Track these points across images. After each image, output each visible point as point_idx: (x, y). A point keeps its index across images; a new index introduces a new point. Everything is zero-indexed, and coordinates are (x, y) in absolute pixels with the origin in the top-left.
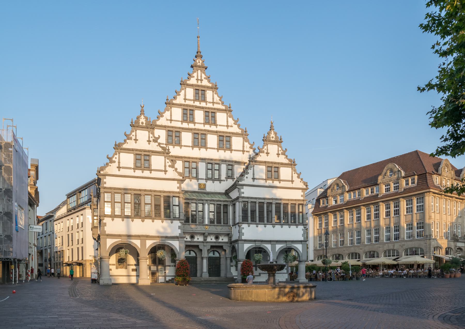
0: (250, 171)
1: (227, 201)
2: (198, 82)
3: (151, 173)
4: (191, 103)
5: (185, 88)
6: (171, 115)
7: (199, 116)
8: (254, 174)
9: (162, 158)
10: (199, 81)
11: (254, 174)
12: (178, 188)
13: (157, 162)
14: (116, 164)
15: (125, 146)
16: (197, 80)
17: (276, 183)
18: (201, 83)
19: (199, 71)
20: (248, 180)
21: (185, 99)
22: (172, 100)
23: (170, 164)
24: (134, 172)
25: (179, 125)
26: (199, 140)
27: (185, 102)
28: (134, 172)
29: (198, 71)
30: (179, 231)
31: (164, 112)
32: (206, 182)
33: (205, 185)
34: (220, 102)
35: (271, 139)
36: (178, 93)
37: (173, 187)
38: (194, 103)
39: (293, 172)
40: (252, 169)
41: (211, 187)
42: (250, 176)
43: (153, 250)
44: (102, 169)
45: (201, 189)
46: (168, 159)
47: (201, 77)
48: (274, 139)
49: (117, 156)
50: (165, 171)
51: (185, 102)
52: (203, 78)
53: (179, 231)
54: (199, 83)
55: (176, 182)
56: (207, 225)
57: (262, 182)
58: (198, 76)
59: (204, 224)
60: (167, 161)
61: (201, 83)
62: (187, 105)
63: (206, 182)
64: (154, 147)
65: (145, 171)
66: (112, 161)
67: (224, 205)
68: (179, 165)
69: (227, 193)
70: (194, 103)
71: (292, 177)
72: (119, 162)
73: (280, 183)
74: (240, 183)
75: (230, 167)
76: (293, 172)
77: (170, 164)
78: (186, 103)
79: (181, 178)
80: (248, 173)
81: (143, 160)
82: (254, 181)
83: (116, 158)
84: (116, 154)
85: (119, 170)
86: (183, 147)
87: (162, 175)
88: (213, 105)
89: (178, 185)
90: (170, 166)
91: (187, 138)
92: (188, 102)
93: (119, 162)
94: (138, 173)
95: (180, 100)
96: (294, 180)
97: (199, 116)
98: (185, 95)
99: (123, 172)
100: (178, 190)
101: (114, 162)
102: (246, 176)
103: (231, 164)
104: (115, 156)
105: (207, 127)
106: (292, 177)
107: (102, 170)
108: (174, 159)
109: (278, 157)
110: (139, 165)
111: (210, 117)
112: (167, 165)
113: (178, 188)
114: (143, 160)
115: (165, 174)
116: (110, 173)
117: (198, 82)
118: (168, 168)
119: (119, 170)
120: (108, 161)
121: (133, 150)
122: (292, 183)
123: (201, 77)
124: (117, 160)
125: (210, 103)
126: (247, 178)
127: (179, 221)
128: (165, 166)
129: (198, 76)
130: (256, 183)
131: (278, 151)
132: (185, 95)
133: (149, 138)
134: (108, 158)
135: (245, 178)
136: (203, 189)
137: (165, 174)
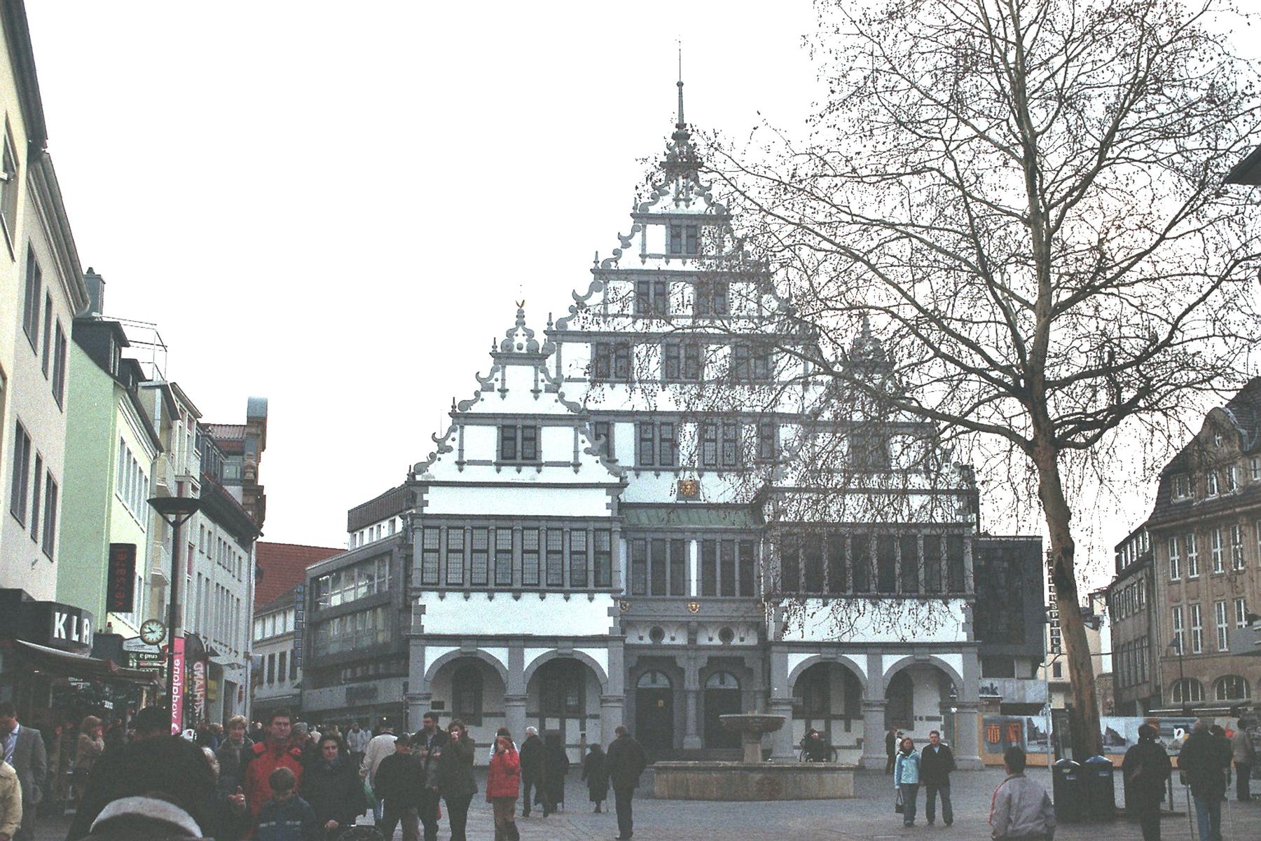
1: (750, 531)
3: (539, 471)
4: (661, 264)
5: (645, 227)
7: (681, 296)
9: (567, 432)
10: (682, 204)
12: (608, 506)
13: (556, 443)
14: (454, 456)
15: (475, 409)
18: (687, 206)
21: (644, 256)
22: (607, 261)
23: (588, 445)
24: (498, 471)
25: (625, 325)
26: (683, 361)
27: (644, 262)
28: (498, 471)
30: (610, 622)
31: (589, 296)
32: (700, 476)
33: (696, 485)
36: (625, 241)
37: (596, 505)
38: (667, 263)
41: (718, 489)
43: (544, 669)
44: (420, 468)
45: (688, 497)
46: (583, 433)
49: (456, 435)
50: (576, 466)
51: (644, 262)
53: (610, 622)
55: (604, 491)
56: (693, 600)
59: (687, 596)
60: (581, 437)
61: (687, 206)
62: (648, 272)
63: (700, 476)
64: (548, 404)
65: (524, 469)
66: (444, 449)
67: (743, 541)
68: (624, 437)
69: (755, 508)
70: (667, 263)
72: (461, 450)
75: (766, 431)
77: (588, 445)
78: (646, 267)
79: (617, 480)
81: (519, 442)
83: (454, 440)
84: (455, 430)
85: (461, 470)
87: (566, 475)
89: (609, 499)
90: (587, 451)
91: (649, 361)
92: (651, 265)
93: (461, 450)
94: (508, 474)
95: (630, 260)
97: (681, 296)
98: (644, 245)
99: (471, 474)
100: (608, 513)
101: (449, 449)
103: (768, 423)
104: (453, 435)
107: (420, 472)
108: (599, 427)
110: (509, 453)
111: (711, 293)
112: (582, 447)
113: (608, 506)
114: (519, 442)
115: (576, 472)
116: (438, 478)
118: (583, 458)
119: (461, 470)
120: (434, 448)
124: (455, 445)
127: (608, 596)
128: (576, 452)
132: (644, 245)
133: (536, 385)
134: (434, 439)
136: (692, 498)
137: (576, 472)
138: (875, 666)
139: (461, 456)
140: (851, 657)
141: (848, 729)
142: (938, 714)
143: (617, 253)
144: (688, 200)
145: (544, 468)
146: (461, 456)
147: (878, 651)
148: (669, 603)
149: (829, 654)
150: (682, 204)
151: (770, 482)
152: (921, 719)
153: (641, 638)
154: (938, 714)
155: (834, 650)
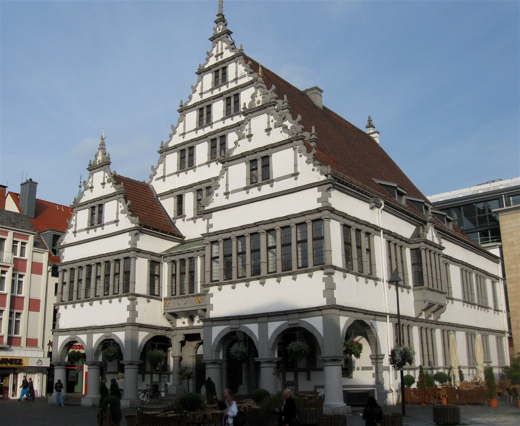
0: (222, 182)
2: (217, 60)
6: (184, 127)
7: (218, 109)
8: (227, 185)
11: (227, 185)
16: (217, 56)
17: (266, 190)
19: (220, 42)
20: (218, 199)
23: (122, 208)
28: (88, 233)
29: (217, 43)
34: (246, 73)
35: (257, 105)
39: (298, 155)
40: (225, 176)
42: (222, 190)
47: (222, 48)
48: (260, 104)
50: (117, 221)
51: (201, 97)
52: (224, 50)
54: (220, 59)
57: (243, 196)
58: (217, 50)
60: (120, 204)
61: (221, 58)
71: (296, 165)
72: (76, 225)
73: (272, 186)
74: (206, 208)
76: (298, 155)
80: (219, 186)
82: (227, 198)
85: (75, 236)
86: (197, 169)
88: (236, 83)
90: (122, 212)
96: (299, 170)
102: (216, 192)
105: (229, 122)
106: (296, 165)
109: (269, 135)
112: (120, 209)
115: (117, 225)
117: (217, 60)
121: (86, 203)
122: (296, 179)
123: (222, 48)
125: (232, 82)
126: (217, 195)
127: (127, 297)
128: (117, 213)
129: (217, 50)
130: (234, 198)
131: (268, 123)
135: (214, 197)
138: (263, 331)
139: (75, 228)
140: (245, 325)
141: (309, 379)
142: (370, 365)
143: (190, 98)
144: (222, 54)
145: (105, 227)
146: (75, 228)
147: (265, 319)
148: (186, 299)
149: (234, 325)
150: (219, 57)
151: (204, 207)
152: (358, 369)
153: (184, 323)
154: (370, 365)
155: (237, 322)
